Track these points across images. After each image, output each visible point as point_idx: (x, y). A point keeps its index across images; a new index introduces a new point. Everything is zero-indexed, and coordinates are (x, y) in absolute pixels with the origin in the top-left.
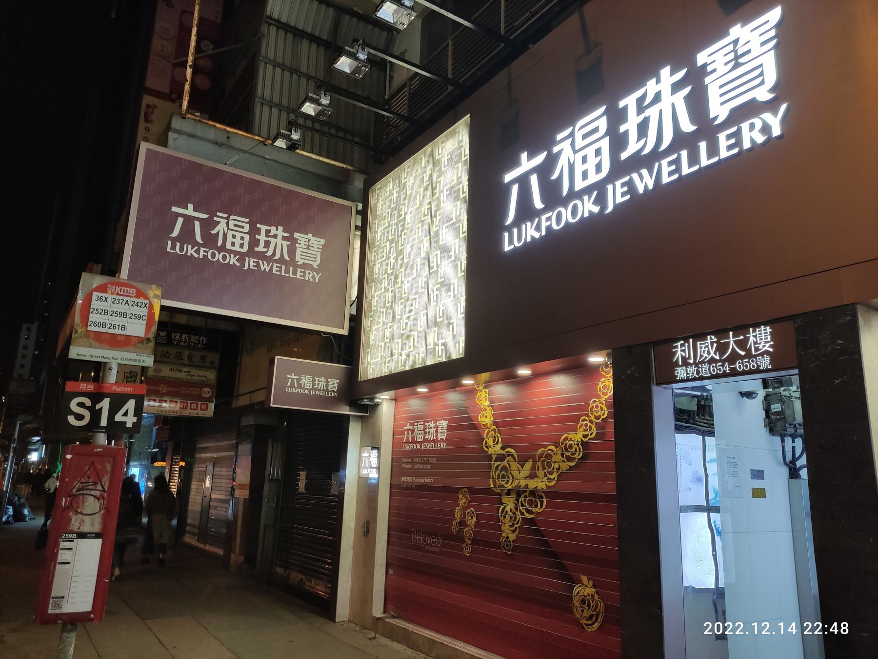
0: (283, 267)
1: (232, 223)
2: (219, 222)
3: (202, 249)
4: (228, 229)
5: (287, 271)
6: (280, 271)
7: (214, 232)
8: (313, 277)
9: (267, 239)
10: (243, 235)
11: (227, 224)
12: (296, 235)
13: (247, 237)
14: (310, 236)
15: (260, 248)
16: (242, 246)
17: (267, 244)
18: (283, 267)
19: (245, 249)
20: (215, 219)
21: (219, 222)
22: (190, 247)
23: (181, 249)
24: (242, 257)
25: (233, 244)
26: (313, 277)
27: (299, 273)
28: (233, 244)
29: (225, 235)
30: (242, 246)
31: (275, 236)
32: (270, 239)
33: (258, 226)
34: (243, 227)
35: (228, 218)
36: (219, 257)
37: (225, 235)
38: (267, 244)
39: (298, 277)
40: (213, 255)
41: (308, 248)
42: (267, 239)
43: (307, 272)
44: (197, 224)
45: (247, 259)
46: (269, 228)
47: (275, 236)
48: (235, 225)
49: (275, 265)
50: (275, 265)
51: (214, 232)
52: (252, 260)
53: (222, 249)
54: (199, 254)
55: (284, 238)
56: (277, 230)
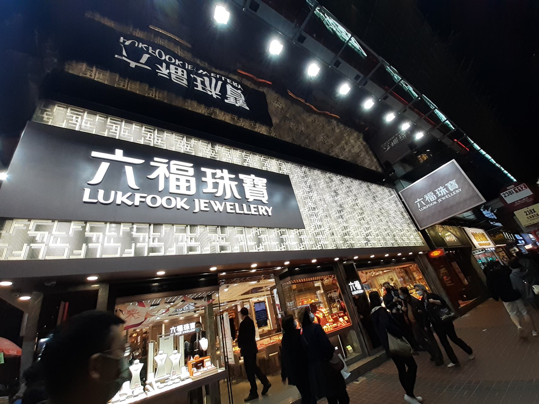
0: (237, 205)
1: (173, 168)
2: (158, 167)
3: (138, 195)
4: (170, 173)
5: (242, 208)
6: (235, 209)
7: (153, 176)
8: (266, 211)
9: (215, 181)
10: (188, 178)
11: (169, 168)
12: (241, 176)
13: (193, 180)
14: (253, 176)
15: (209, 189)
16: (188, 188)
17: (216, 185)
18: (237, 205)
19: (193, 191)
20: (152, 163)
21: (158, 167)
22: (120, 193)
23: (106, 197)
24: (190, 199)
25: (178, 187)
26: (266, 211)
27: (253, 210)
28: (178, 187)
29: (167, 179)
30: (188, 188)
31: (222, 178)
32: (218, 181)
33: (203, 169)
34: (187, 171)
35: (168, 163)
36: (161, 201)
37: (167, 179)
38: (216, 185)
39: (253, 213)
40: (154, 199)
41: (254, 187)
42: (215, 181)
43: (260, 207)
44: (129, 170)
45: (197, 201)
46: (214, 171)
47: (222, 178)
48: (177, 169)
49: (228, 204)
50: (228, 204)
51: (153, 176)
52: (202, 201)
53: (166, 192)
54: (133, 200)
55: (231, 179)
56: (222, 172)
